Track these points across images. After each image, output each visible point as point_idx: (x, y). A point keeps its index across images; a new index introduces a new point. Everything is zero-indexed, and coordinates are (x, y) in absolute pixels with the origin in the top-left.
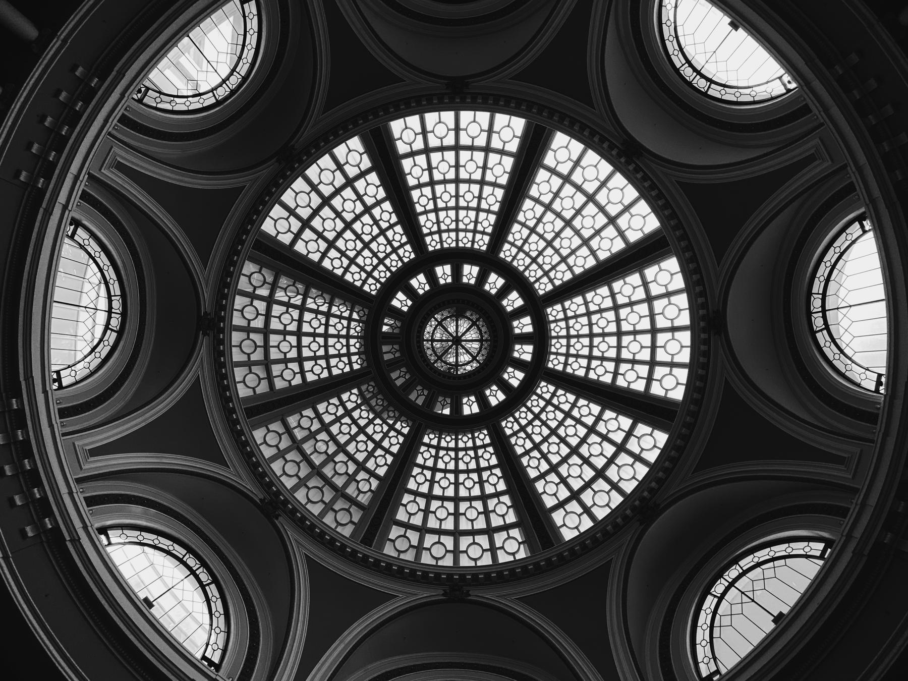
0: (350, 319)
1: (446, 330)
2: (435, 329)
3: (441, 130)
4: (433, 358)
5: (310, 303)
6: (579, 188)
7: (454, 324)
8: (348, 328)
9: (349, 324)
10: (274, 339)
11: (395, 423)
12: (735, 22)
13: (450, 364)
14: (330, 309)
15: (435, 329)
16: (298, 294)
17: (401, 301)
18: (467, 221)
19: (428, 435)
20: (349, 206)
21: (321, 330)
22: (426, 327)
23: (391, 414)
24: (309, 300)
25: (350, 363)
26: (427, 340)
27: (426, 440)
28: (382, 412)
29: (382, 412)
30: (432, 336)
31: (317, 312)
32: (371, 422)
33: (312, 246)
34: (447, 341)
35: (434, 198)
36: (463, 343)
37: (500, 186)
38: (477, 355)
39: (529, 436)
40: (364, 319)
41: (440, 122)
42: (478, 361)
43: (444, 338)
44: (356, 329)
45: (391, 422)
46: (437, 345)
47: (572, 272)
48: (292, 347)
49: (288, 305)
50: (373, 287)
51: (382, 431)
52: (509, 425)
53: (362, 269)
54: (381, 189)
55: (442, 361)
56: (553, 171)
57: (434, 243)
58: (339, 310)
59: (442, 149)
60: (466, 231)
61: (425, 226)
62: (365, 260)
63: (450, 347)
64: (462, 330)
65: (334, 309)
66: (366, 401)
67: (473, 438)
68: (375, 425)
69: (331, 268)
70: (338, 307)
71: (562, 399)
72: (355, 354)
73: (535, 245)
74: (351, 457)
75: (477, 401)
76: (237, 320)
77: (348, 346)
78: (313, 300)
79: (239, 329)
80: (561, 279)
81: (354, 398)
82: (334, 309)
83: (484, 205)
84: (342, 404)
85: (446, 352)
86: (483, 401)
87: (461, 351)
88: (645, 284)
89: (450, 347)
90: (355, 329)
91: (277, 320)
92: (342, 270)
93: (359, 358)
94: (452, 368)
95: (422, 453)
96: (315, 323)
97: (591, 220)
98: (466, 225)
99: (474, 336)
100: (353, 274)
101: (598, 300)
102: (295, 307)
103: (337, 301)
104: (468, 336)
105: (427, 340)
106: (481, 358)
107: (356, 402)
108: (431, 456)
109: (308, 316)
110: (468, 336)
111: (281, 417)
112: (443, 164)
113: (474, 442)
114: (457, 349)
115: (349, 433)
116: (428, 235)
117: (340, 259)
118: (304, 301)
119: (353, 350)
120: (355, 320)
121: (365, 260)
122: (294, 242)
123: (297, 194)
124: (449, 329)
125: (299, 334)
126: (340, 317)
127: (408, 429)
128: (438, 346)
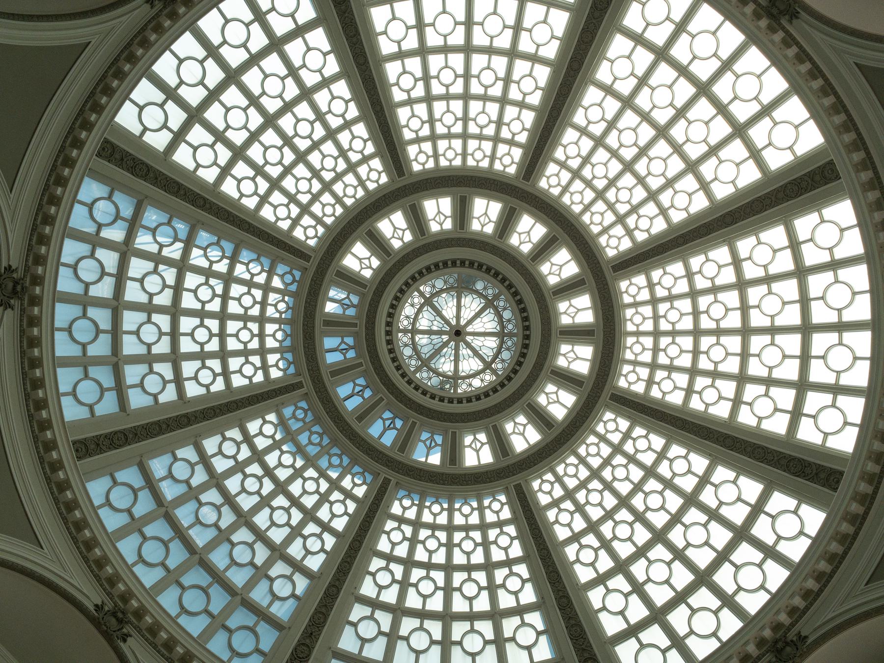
0: (267, 288)
1: (439, 313)
2: (420, 311)
4: (413, 362)
5: (197, 258)
6: (683, 71)
9: (265, 297)
11: (341, 477)
13: (443, 375)
14: (231, 268)
15: (420, 311)
16: (176, 239)
17: (360, 259)
18: (483, 120)
19: (400, 500)
20: (273, 86)
21: (215, 306)
22: (403, 308)
23: (335, 461)
24: (196, 252)
25: (265, 367)
26: (405, 331)
27: (396, 509)
28: (319, 456)
29: (319, 456)
30: (414, 324)
31: (208, 273)
32: (298, 473)
33: (205, 156)
34: (440, 333)
35: (426, 78)
37: (543, 61)
38: (493, 361)
39: (580, 509)
40: (293, 288)
42: (494, 372)
43: (435, 328)
44: (277, 306)
45: (334, 475)
46: (422, 340)
47: (667, 219)
49: (157, 259)
50: (311, 232)
51: (317, 491)
52: (546, 487)
54: (331, 58)
55: (430, 369)
57: (422, 158)
58: (248, 270)
61: (407, 126)
65: (240, 270)
66: (290, 436)
67: (481, 509)
68: (305, 480)
69: (236, 195)
70: (247, 265)
71: (642, 444)
72: (273, 351)
74: (260, 536)
75: (490, 442)
76: (66, 283)
77: (262, 336)
78: (202, 252)
79: (69, 298)
81: (268, 430)
82: (240, 270)
84: (248, 439)
85: (437, 352)
86: (500, 443)
87: (464, 351)
88: (795, 245)
89: (445, 345)
90: (275, 306)
91: (137, 285)
92: (255, 200)
93: (282, 358)
94: (447, 382)
95: (388, 533)
98: (482, 128)
100: (275, 207)
102: (169, 262)
103: (245, 255)
104: (477, 326)
105: (405, 331)
106: (500, 366)
107: (272, 437)
108: (405, 538)
110: (477, 326)
111: (139, 459)
113: (482, 516)
114: (457, 349)
115: (258, 493)
117: (253, 179)
118: (186, 252)
119: (270, 343)
120: (276, 290)
122: (172, 146)
124: (444, 312)
126: (250, 284)
127: (364, 488)
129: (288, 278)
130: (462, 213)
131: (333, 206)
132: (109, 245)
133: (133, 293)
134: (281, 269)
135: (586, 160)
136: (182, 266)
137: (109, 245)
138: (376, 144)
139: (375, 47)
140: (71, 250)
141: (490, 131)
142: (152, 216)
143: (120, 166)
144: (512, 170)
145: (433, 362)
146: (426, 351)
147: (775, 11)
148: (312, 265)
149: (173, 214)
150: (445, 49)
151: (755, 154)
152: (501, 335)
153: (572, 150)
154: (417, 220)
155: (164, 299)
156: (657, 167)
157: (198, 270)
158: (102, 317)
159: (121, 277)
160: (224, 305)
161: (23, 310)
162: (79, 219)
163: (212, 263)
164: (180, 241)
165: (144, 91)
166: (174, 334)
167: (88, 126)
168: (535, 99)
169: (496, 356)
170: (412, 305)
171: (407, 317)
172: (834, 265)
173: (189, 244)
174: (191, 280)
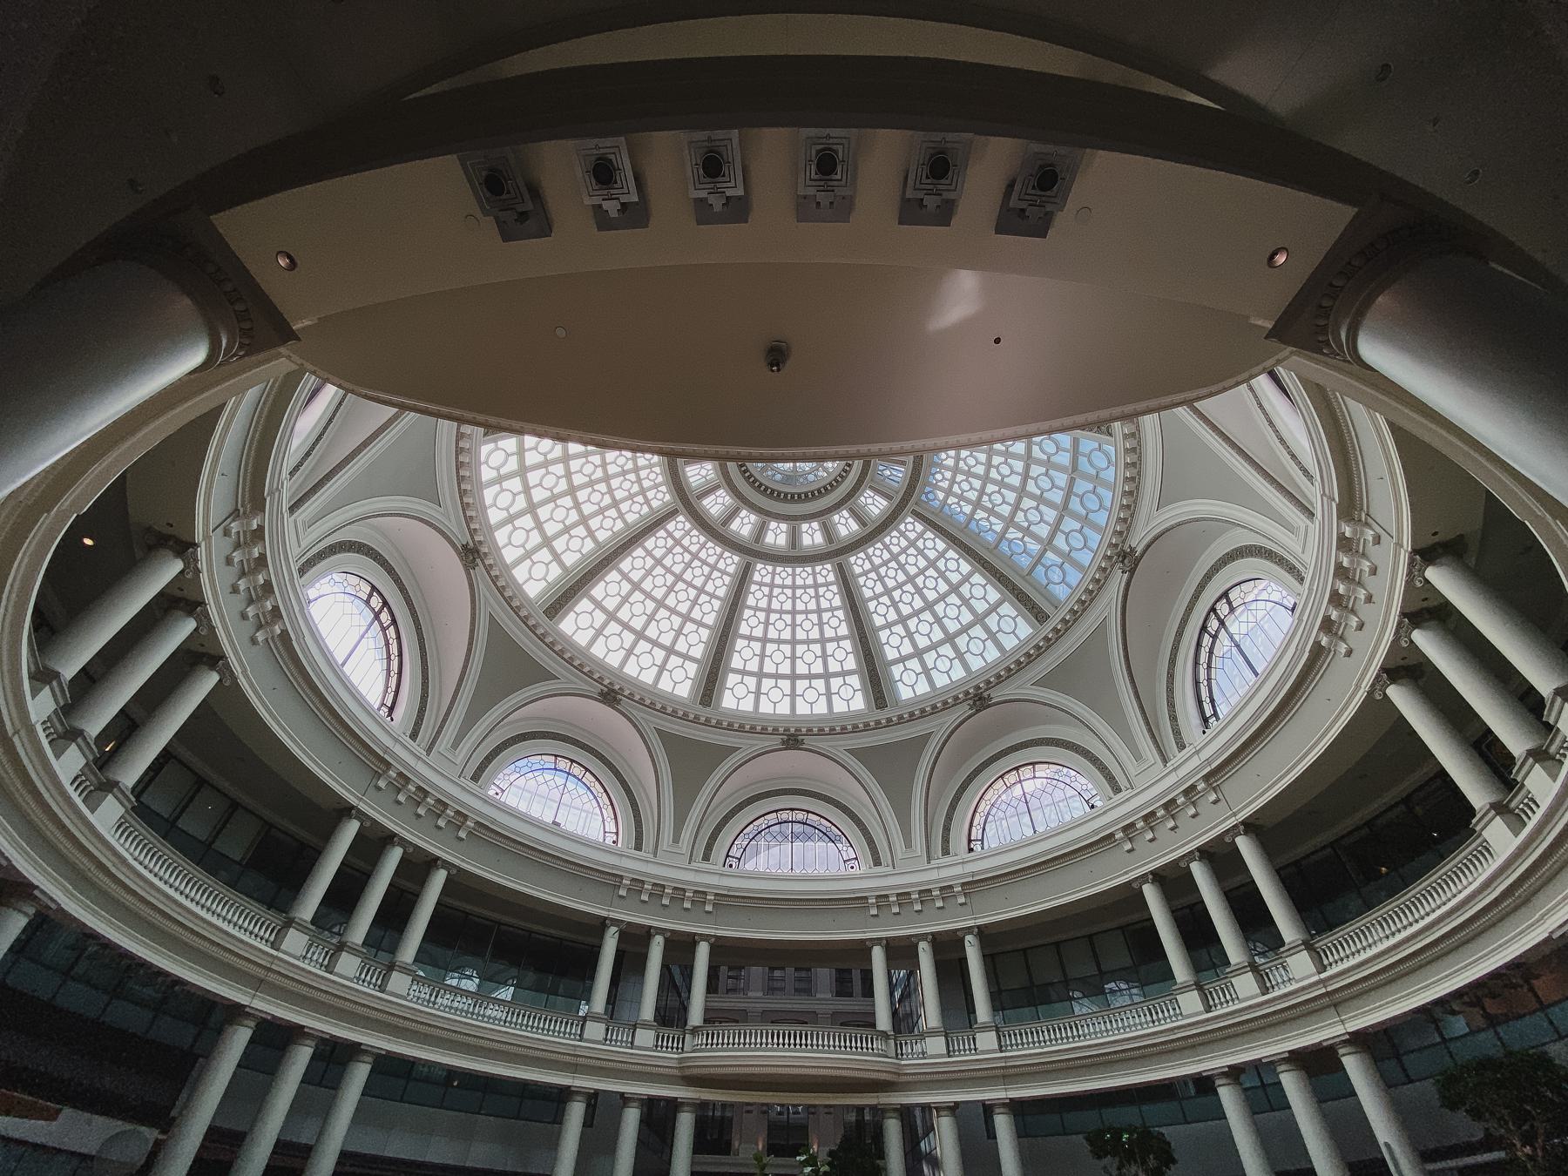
3: (811, 695)
12: (556, 827)
14: (973, 512)
16: (1010, 541)
24: (998, 528)
31: (991, 512)
40: (928, 489)
41: (811, 704)
48: (1035, 479)
49: (1027, 531)
50: (910, 527)
53: (921, 552)
56: (686, 657)
58: (961, 507)
59: (810, 677)
62: (914, 563)
65: (967, 509)
73: (696, 575)
76: (1094, 538)
79: (1095, 527)
88: (557, 557)
96: (997, 499)
97: (635, 612)
98: (783, 593)
101: (608, 523)
109: (1005, 510)
112: (809, 660)
118: (1005, 530)
120: (941, 489)
121: (914, 563)
122: (999, 604)
123: (981, 654)
126: (961, 497)
129: (931, 496)
130: (794, 537)
131: (886, 575)
132: (1058, 552)
133: (1050, 515)
135: (708, 577)
136: (1010, 522)
137: (1058, 552)
138: (857, 583)
139: (854, 646)
140: (1085, 558)
141: (776, 591)
142: (1025, 562)
143: (1035, 603)
144: (759, 566)
147: (613, 694)
148: (911, 506)
150: (808, 642)
151: (598, 605)
153: (719, 582)
156: (659, 581)
157: (998, 516)
158: (1075, 504)
159: (1056, 528)
161: (1124, 542)
162: (1074, 577)
164: (1007, 539)
165: (1010, 643)
166: (1026, 477)
167: (1046, 639)
168: (747, 613)
172: (528, 555)
173: (1002, 536)
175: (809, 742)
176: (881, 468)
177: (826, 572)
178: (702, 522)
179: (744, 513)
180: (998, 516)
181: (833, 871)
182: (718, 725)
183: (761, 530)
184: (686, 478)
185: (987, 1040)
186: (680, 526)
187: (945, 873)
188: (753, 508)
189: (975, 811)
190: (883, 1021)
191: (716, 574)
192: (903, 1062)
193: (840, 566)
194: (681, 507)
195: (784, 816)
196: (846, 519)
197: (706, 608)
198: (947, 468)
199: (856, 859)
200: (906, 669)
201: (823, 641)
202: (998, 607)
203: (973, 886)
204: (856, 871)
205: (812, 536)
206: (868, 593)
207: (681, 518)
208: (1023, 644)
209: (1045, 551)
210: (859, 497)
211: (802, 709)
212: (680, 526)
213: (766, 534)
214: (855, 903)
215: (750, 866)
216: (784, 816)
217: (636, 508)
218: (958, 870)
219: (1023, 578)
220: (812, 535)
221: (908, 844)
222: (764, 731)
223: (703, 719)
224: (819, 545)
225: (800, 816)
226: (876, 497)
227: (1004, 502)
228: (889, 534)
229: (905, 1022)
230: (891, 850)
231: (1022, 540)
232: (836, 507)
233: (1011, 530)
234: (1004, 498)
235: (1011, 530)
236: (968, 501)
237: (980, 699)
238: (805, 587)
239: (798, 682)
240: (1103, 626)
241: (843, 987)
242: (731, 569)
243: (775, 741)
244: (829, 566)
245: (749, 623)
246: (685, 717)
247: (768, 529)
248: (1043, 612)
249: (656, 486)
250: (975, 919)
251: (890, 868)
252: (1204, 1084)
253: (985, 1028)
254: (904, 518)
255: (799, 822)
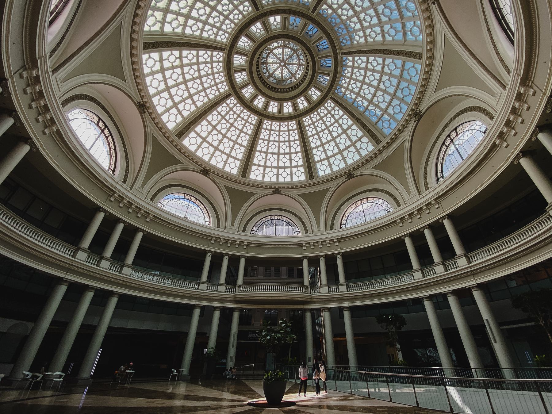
1: (289, 71)
2: (296, 72)
4: (300, 53)
6: (223, 152)
7: (284, 74)
8: (349, 84)
10: (392, 90)
14: (356, 98)
15: (296, 72)
16: (370, 110)
21: (365, 86)
24: (365, 105)
25: (353, 61)
26: (302, 65)
31: (364, 98)
34: (289, 64)
36: (278, 62)
38: (269, 53)
40: (338, 87)
41: (285, 178)
43: (291, 65)
44: (344, 82)
46: (296, 61)
47: (218, 111)
48: (384, 82)
49: (377, 106)
50: (329, 105)
55: (293, 50)
60: (275, 131)
61: (296, 134)
62: (329, 120)
63: (287, 59)
64: (279, 71)
65: (354, 96)
73: (239, 124)
80: (223, 107)
83: (266, 143)
87: (280, 56)
89: (287, 59)
96: (367, 91)
98: (275, 133)
99: (272, 66)
103: (351, 101)
104: (275, 66)
105: (302, 65)
114: (283, 57)
116: (295, 130)
118: (368, 106)
119: (350, 70)
120: (344, 87)
121: (329, 120)
124: (287, 71)
125: (377, 88)
126: (352, 91)
128: (295, 61)
129: (339, 91)
130: (281, 108)
134: (341, 94)
137: (389, 115)
138: (305, 129)
139: (303, 155)
140: (399, 117)
144: (266, 121)
145: (292, 53)
146: (295, 56)
148: (331, 95)
149: (368, 119)
152: (266, 63)
154: (295, 106)
155: (379, 93)
157: (366, 99)
158: (399, 94)
160: (362, 86)
163: (362, 101)
164: (368, 110)
169: (268, 55)
170: (299, 74)
171: (301, 70)
174: (369, 97)
175: (283, 191)
176: (319, 77)
177: (293, 125)
178: (241, 100)
179: (260, 97)
180: (366, 99)
181: (290, 235)
182: (249, 185)
183: (267, 105)
184: (235, 79)
185: (343, 289)
186: (232, 102)
187: (331, 235)
188: (264, 95)
189: (344, 215)
190: (306, 282)
191: (247, 124)
192: (313, 295)
193: (299, 122)
194: (233, 93)
195: (273, 217)
196: (303, 101)
197: (244, 139)
198: (347, 78)
199: (299, 231)
200: (322, 164)
201: (290, 153)
202: (361, 139)
203: (341, 240)
204: (299, 235)
205: (288, 108)
206: (309, 134)
207: (233, 98)
208: (369, 153)
209: (383, 114)
210: (308, 91)
211: (281, 180)
212: (232, 102)
213: (269, 106)
214: (298, 246)
215: (260, 234)
216: (273, 217)
217: (213, 92)
218: (336, 234)
219: (373, 126)
220: (288, 109)
221: (318, 226)
222: (266, 187)
223: (242, 182)
224: (291, 113)
225: (279, 217)
226: (316, 91)
227: (369, 93)
228: (320, 108)
229: (313, 284)
230: (312, 229)
231: (375, 110)
232: (298, 96)
233: (371, 105)
234: (369, 91)
235: (371, 105)
236: (354, 93)
237: (350, 175)
238: (284, 131)
239: (280, 170)
240: (402, 145)
241: (290, 274)
242: (254, 122)
243: (271, 191)
244: (294, 122)
245: (261, 146)
246: (235, 181)
247: (269, 105)
248: (379, 140)
249: (222, 82)
250: (341, 250)
251: (311, 234)
252: (418, 302)
253: (342, 285)
254: (327, 100)
255: (278, 219)
